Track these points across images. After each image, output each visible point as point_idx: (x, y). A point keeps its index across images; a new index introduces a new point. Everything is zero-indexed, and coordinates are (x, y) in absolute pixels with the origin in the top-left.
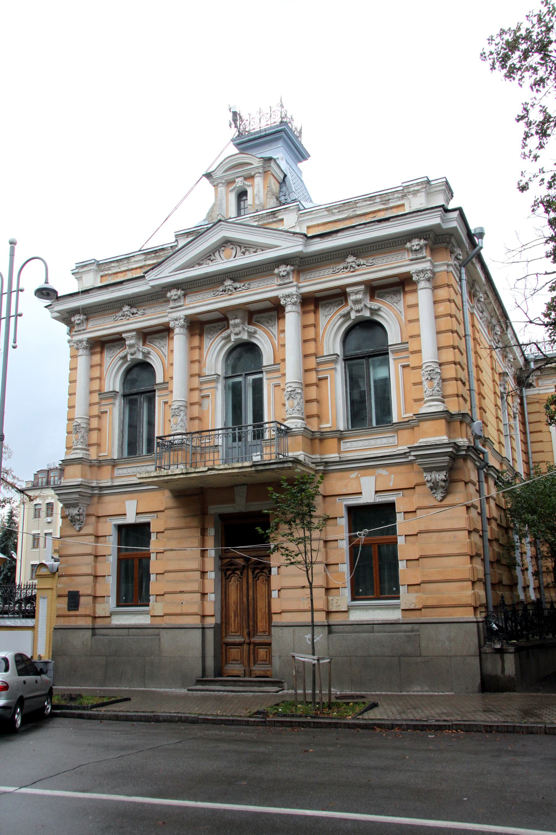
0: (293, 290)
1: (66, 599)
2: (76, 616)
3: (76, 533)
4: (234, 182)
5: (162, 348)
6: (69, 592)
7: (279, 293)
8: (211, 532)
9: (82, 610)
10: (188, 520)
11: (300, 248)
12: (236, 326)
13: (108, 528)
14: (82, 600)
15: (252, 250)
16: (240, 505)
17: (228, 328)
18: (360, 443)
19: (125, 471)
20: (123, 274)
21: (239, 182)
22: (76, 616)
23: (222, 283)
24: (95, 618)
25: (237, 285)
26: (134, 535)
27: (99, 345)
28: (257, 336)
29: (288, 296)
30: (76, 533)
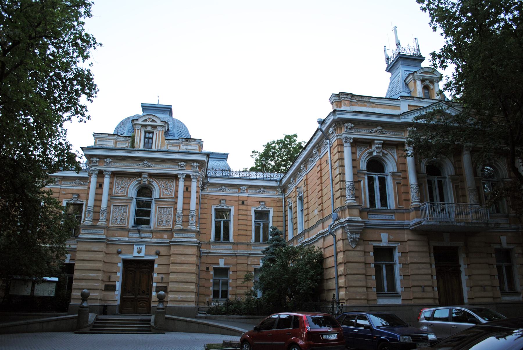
8: (432, 255)
13: (370, 248)
16: (447, 243)
18: (379, 217)
24: (368, 300)
26: (384, 254)
27: (356, 143)
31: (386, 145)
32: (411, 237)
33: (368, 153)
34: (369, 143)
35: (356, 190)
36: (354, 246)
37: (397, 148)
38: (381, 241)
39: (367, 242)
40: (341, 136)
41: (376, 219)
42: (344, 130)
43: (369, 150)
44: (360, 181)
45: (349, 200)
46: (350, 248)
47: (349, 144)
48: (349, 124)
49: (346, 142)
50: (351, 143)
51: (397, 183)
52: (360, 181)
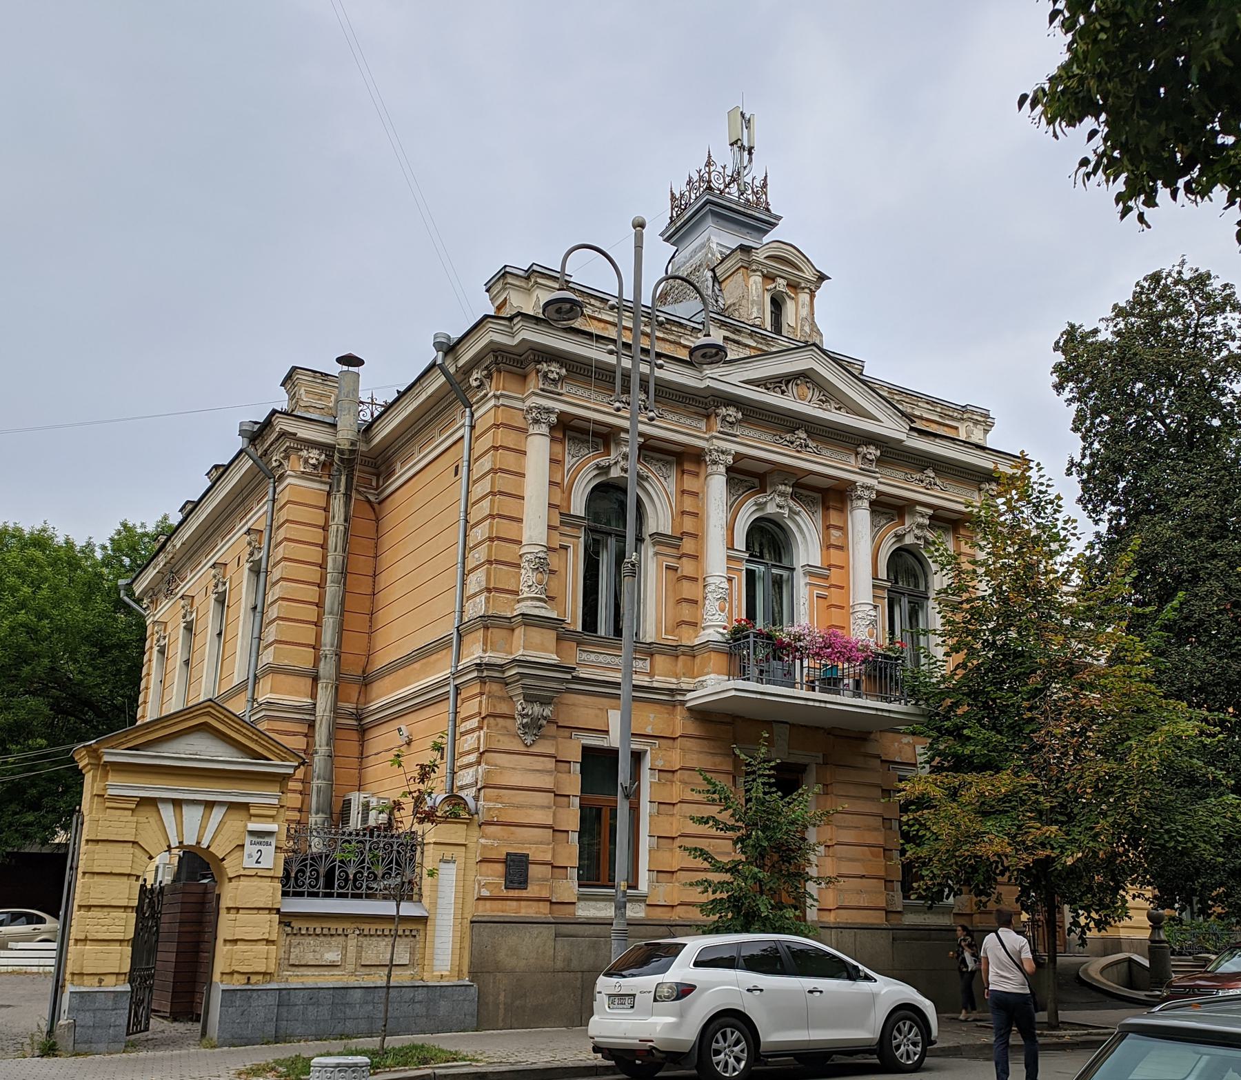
0: (874, 482)
1: (500, 868)
2: (519, 899)
3: (523, 749)
4: (773, 280)
5: (662, 479)
6: (508, 854)
7: (861, 480)
9: (532, 890)
10: (718, 759)
11: (903, 437)
12: (782, 494)
14: (533, 870)
15: (833, 405)
17: (763, 490)
19: (593, 657)
20: (602, 325)
21: (781, 284)
22: (519, 899)
23: (792, 431)
25: (810, 443)
27: (568, 430)
28: (797, 518)
29: (868, 488)
30: (523, 749)
31: (652, 450)
32: (692, 729)
33: (598, 467)
34: (605, 437)
35: (552, 572)
36: (529, 742)
37: (680, 464)
38: (607, 732)
39: (566, 733)
40: (523, 401)
41: (595, 664)
42: (534, 384)
43: (603, 461)
44: (566, 548)
45: (532, 599)
46: (517, 746)
47: (544, 429)
48: (554, 367)
49: (536, 421)
50: (552, 428)
51: (668, 567)
52: (566, 548)
